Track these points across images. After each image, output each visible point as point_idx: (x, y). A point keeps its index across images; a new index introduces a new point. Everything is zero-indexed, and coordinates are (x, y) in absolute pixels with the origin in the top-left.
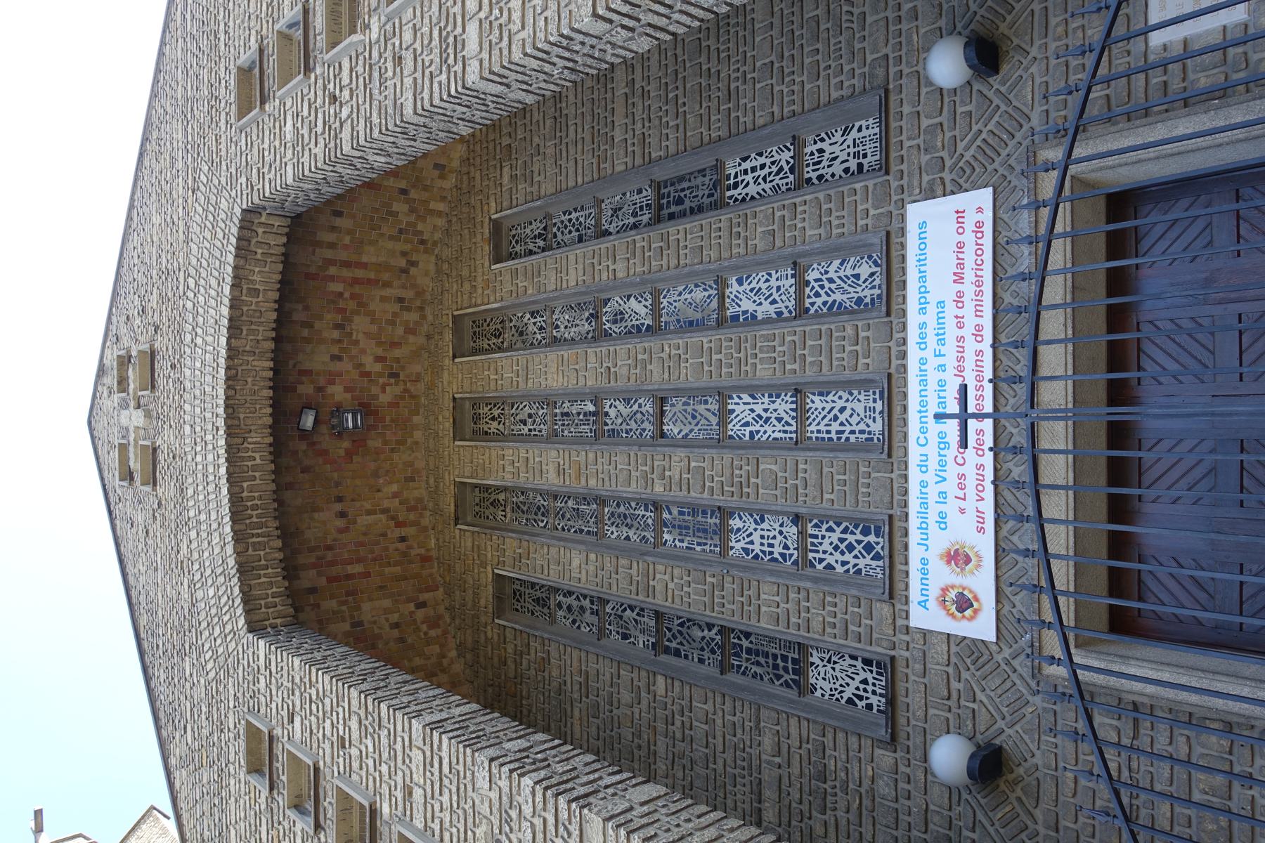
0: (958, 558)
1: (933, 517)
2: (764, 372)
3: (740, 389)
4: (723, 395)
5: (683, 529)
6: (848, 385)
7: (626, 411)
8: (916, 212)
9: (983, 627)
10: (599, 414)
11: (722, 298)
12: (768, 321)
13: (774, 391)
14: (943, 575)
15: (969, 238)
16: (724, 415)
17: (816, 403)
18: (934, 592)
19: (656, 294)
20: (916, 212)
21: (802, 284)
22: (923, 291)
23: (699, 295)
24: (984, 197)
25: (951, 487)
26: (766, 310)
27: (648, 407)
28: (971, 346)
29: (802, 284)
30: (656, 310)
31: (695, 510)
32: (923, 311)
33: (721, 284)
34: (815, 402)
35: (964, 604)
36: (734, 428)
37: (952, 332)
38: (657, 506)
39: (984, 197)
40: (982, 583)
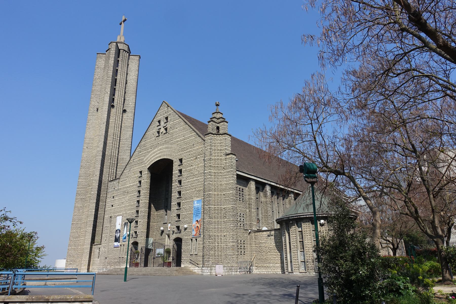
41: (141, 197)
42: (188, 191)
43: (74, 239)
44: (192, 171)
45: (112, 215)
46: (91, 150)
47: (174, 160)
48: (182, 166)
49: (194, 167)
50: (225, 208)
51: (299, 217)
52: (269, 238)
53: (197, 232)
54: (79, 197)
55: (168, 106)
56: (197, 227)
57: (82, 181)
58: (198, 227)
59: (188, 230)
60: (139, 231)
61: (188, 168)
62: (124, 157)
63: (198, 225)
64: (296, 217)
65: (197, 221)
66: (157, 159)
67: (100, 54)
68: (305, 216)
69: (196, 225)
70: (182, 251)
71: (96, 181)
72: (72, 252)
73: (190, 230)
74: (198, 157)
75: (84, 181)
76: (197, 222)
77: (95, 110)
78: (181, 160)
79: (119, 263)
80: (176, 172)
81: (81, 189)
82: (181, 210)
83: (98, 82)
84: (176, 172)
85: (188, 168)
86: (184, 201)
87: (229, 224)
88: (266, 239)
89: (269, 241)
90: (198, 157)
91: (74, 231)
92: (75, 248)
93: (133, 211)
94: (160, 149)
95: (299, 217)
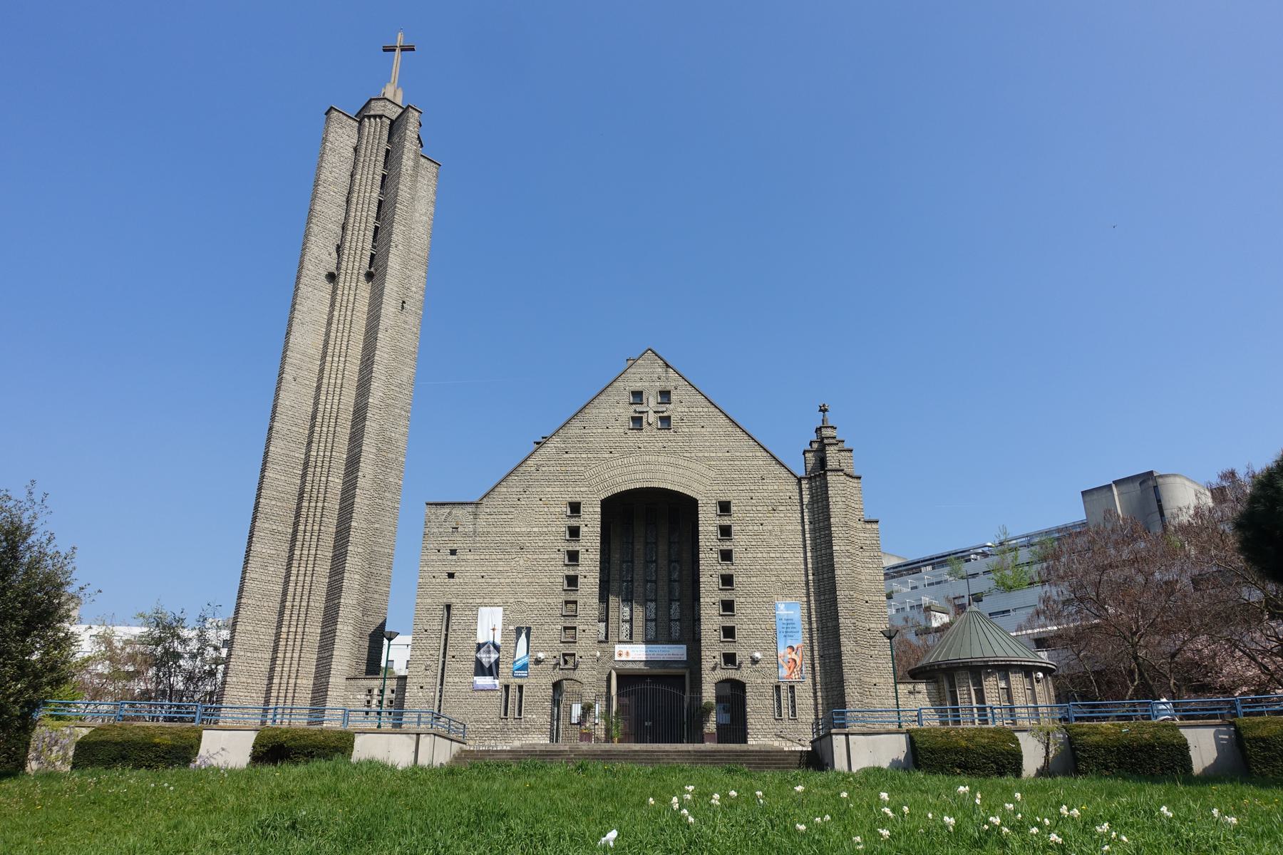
0: (627, 654)
1: (634, 649)
2: (660, 613)
3: (656, 605)
4: (655, 600)
5: (627, 588)
6: (656, 631)
7: (653, 571)
8: (685, 647)
9: (617, 658)
10: (652, 562)
11: (676, 600)
12: (670, 612)
13: (656, 614)
14: (624, 651)
15: (679, 656)
16: (651, 601)
17: (654, 623)
18: (621, 649)
19: (678, 581)
20: (685, 647)
21: (676, 620)
22: (671, 648)
23: (677, 594)
24: (685, 659)
25: (639, 653)
26: (672, 611)
27: (654, 578)
28: (662, 657)
29: (676, 620)
30: (675, 581)
31: (632, 592)
32: (669, 648)
33: (678, 600)
34: (654, 623)
35: (620, 655)
36: (649, 603)
37: (664, 653)
38: (632, 581)
39: (685, 659)
40: (624, 658)
41: (580, 568)
42: (754, 579)
43: (249, 654)
44: (765, 537)
45: (453, 600)
46: (304, 390)
47: (702, 500)
48: (730, 519)
49: (770, 528)
50: (872, 629)
51: (1008, 663)
52: (912, 696)
53: (793, 672)
54: (266, 525)
55: (668, 366)
56: (791, 661)
57: (279, 477)
58: (795, 661)
59: (764, 665)
60: (582, 654)
61: (751, 528)
62: (393, 435)
63: (793, 655)
64: (1003, 663)
65: (791, 647)
66: (638, 486)
67: (341, 114)
68: (1019, 663)
69: (789, 656)
70: (748, 710)
71: (365, 492)
72: (240, 694)
73: (768, 666)
74: (781, 508)
75: (283, 478)
76: (789, 650)
77: (319, 274)
78: (725, 507)
79: (502, 731)
80: (711, 528)
81: (273, 503)
82: (736, 617)
83: (332, 193)
84: (711, 528)
85: (751, 528)
86: (742, 600)
87: (884, 662)
88: (905, 699)
89: (911, 703)
90: (781, 508)
91: (248, 628)
92: (249, 681)
93: (549, 601)
94: (648, 463)
95: (1008, 663)
